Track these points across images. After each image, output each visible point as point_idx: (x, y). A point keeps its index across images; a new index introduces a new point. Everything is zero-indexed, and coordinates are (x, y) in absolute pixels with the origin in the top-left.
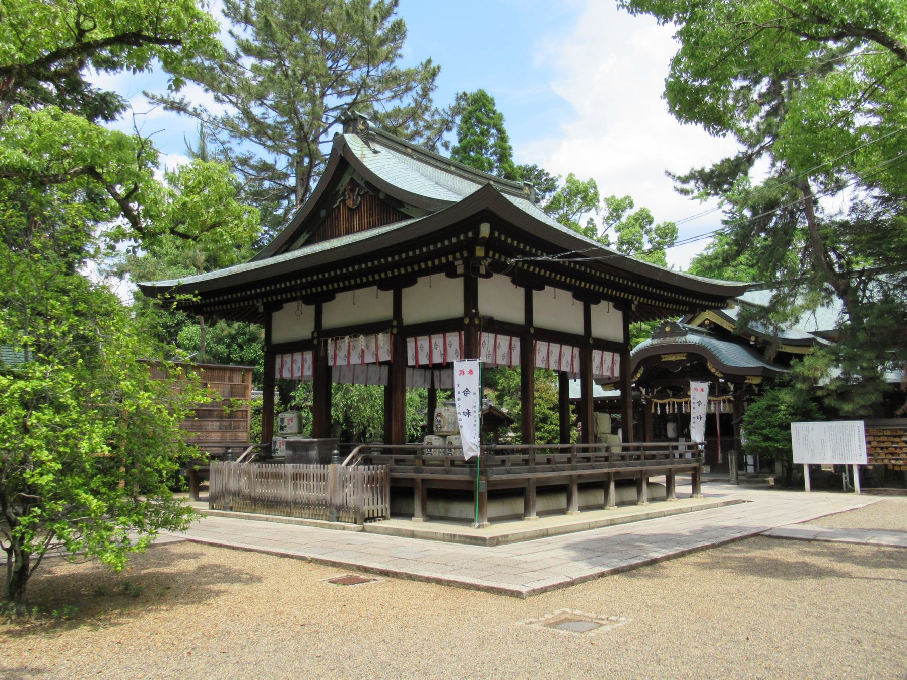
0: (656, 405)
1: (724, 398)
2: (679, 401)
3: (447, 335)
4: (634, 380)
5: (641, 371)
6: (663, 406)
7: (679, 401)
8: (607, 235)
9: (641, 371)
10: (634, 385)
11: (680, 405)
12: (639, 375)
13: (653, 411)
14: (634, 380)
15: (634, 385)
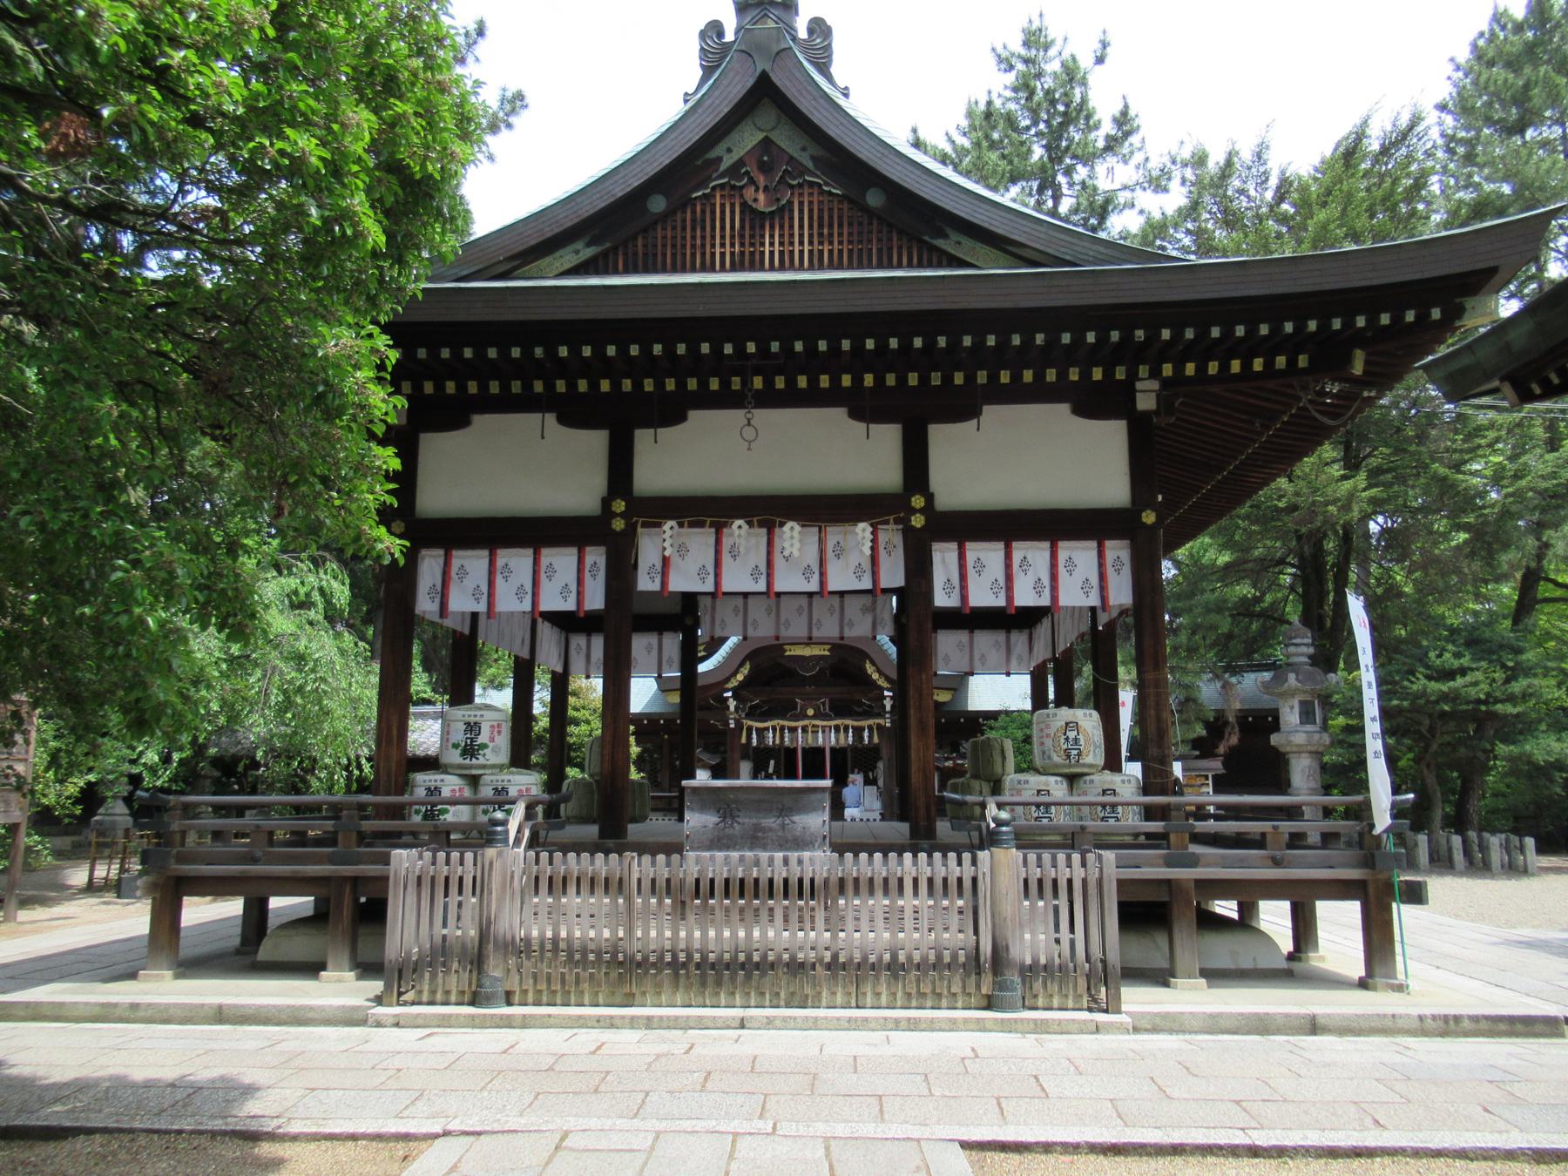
0: (750, 729)
1: (871, 722)
2: (793, 724)
3: (545, 552)
4: (730, 685)
5: (746, 670)
7: (793, 724)
13: (744, 740)
14: (730, 685)
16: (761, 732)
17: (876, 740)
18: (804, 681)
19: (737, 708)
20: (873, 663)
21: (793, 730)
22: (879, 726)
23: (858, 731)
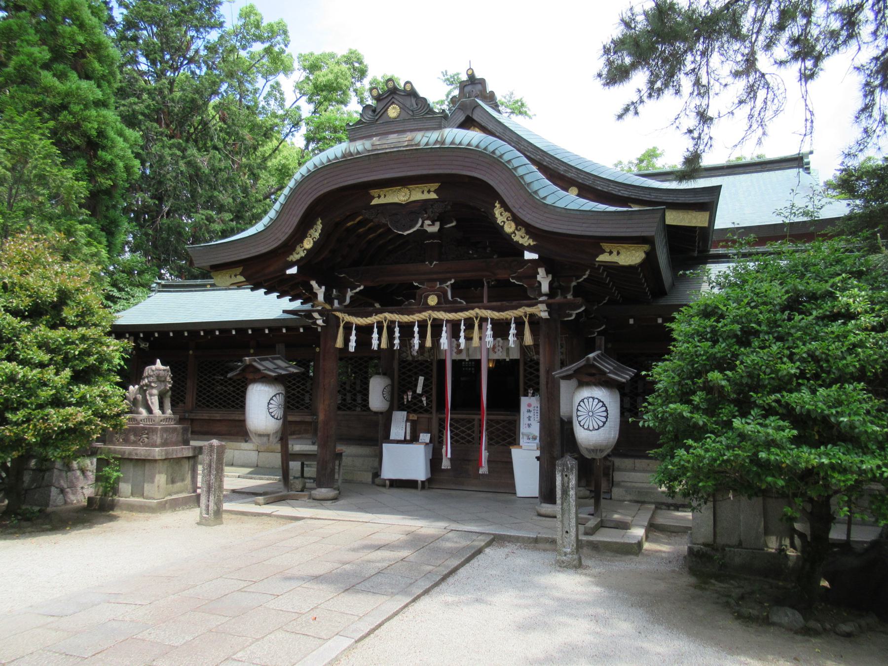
0: (348, 327)
1: (520, 312)
2: (406, 318)
4: (295, 257)
5: (316, 233)
6: (365, 332)
7: (406, 318)
8: (298, 108)
9: (316, 233)
10: (293, 270)
11: (406, 329)
12: (308, 244)
13: (339, 343)
14: (295, 257)
15: (293, 270)
16: (365, 332)
17: (528, 339)
20: (505, 207)
21: (406, 329)
22: (532, 316)
23: (501, 329)
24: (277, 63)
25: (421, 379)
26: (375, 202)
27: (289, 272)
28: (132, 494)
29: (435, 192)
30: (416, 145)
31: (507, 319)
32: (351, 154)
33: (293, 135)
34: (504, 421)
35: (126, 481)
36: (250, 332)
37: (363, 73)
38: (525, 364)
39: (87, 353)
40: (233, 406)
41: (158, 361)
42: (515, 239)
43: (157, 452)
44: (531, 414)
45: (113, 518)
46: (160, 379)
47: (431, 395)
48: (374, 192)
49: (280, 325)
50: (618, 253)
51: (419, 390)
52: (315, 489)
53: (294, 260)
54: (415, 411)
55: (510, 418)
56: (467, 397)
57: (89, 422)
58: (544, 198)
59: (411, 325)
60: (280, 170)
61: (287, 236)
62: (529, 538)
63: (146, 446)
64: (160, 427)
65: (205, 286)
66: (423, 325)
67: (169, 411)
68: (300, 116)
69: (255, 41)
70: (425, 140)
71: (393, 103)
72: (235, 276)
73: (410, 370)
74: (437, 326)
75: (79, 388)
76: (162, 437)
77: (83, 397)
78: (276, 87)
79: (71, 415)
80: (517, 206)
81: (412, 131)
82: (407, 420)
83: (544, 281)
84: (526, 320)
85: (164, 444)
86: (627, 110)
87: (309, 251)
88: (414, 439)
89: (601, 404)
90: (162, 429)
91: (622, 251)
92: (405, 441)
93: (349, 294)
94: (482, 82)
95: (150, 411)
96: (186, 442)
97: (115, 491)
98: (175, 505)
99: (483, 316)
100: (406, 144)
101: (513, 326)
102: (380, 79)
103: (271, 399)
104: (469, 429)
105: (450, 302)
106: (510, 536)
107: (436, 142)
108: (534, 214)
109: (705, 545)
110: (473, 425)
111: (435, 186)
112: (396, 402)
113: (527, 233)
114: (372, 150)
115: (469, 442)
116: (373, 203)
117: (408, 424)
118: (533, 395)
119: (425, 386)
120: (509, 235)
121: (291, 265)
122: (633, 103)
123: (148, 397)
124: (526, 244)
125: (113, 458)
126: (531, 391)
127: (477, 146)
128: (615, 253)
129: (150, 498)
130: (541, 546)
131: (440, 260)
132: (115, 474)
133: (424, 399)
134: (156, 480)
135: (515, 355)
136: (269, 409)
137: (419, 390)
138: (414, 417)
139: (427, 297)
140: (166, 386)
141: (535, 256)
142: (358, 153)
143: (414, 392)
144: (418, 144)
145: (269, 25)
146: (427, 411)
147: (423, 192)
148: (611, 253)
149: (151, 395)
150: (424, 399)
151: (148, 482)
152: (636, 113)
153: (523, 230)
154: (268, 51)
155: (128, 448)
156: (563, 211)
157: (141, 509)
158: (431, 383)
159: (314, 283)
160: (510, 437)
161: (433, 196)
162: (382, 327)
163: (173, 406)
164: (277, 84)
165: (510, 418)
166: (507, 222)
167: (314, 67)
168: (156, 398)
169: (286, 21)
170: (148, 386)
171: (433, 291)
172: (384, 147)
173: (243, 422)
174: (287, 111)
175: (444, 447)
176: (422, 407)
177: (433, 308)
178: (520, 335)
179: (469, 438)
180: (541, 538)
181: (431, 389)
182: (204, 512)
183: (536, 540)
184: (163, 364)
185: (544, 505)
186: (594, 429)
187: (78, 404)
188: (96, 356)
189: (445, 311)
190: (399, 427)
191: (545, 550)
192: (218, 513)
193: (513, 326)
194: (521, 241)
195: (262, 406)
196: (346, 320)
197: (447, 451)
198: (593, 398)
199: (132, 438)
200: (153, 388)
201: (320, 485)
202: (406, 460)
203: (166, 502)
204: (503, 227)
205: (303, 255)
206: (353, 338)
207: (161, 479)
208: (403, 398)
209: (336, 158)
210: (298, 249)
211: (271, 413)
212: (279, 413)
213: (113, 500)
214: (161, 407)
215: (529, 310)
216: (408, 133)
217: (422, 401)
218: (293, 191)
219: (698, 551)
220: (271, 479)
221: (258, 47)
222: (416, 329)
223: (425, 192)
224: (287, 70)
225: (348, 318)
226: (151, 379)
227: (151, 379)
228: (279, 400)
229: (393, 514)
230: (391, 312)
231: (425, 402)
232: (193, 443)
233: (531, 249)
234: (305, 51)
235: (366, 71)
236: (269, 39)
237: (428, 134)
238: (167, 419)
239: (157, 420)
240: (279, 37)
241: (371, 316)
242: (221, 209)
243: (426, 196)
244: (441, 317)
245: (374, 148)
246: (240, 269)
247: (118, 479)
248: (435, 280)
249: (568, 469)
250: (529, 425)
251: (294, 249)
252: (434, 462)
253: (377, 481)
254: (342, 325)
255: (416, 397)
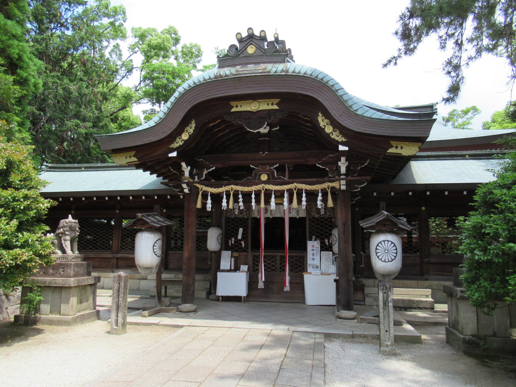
1: (325, 185)
2: (246, 189)
4: (175, 145)
5: (191, 129)
6: (217, 199)
7: (246, 189)
8: (131, 61)
9: (191, 129)
10: (174, 154)
11: (247, 196)
12: (185, 136)
13: (199, 205)
14: (175, 145)
15: (174, 154)
16: (217, 199)
17: (330, 203)
18: (257, 143)
19: (191, 173)
20: (327, 115)
21: (247, 196)
22: (333, 188)
23: (312, 196)
24: (118, 32)
25: (241, 230)
26: (234, 110)
27: (171, 155)
28: (51, 312)
29: (277, 104)
30: (268, 72)
31: (316, 190)
32: (221, 76)
33: (127, 77)
34: (296, 256)
35: (46, 302)
36: (119, 198)
37: (177, 41)
38: (310, 220)
39: (28, 208)
40: (103, 249)
41: (70, 216)
42: (333, 137)
43: (72, 281)
44: (315, 252)
45: (39, 331)
46: (71, 229)
47: (248, 240)
48: (233, 103)
49: (141, 194)
50: (402, 148)
51: (240, 237)
52: (180, 304)
53: (175, 147)
54: (236, 251)
55: (300, 254)
56: (275, 240)
57: (30, 260)
58: (356, 110)
59: (249, 194)
60: (126, 97)
61: (172, 130)
62: (348, 335)
63: (62, 277)
64: (73, 263)
65: (81, 168)
66: (258, 194)
67: (77, 252)
68: (133, 66)
69: (104, 17)
70: (274, 70)
71: (251, 44)
72: (130, 157)
73: (233, 224)
74: (268, 194)
75: (23, 235)
76: (74, 270)
77: (26, 241)
78: (117, 46)
79: (19, 254)
80: (338, 115)
81: (264, 63)
82: (232, 257)
83: (343, 165)
84: (329, 191)
85: (76, 275)
86: (390, 61)
87: (186, 141)
88: (237, 269)
89: (393, 245)
90: (74, 264)
91: (404, 146)
92: (230, 271)
93: (205, 172)
94: (283, 43)
95: (64, 251)
96: (89, 274)
97: (37, 310)
98: (83, 319)
99: (300, 188)
100: (261, 71)
101: (320, 195)
102: (188, 45)
103: (155, 243)
104: (273, 262)
105: (276, 179)
106: (335, 334)
107: (282, 71)
108: (349, 121)
109: (473, 336)
110: (276, 260)
111: (277, 101)
112: (225, 246)
113: (341, 133)
114: (236, 75)
115: (273, 270)
116: (233, 110)
117: (233, 259)
118: (315, 240)
119: (243, 234)
120: (328, 135)
121: (172, 150)
122: (394, 57)
123: (63, 242)
124: (340, 141)
125: (37, 286)
126: (314, 238)
127: (311, 75)
128: (400, 147)
129: (66, 315)
130: (356, 340)
131: (269, 151)
132: (38, 298)
133: (243, 243)
134: (71, 301)
135: (302, 214)
136: (154, 249)
137: (240, 237)
138: (236, 254)
139: (260, 175)
140: (75, 233)
141: (346, 148)
142: (226, 76)
143: (236, 238)
144: (269, 72)
145: (114, 7)
146: (244, 250)
147: (268, 105)
148: (397, 147)
149: (65, 240)
150: (243, 243)
151: (64, 303)
152: (396, 64)
153: (338, 131)
154: (112, 24)
155: (48, 279)
156: (369, 119)
157: (59, 323)
158: (248, 232)
159: (184, 164)
160: (300, 266)
161: (276, 107)
162: (230, 195)
163: (79, 249)
164: (118, 44)
165: (300, 254)
166: (327, 126)
167: (142, 37)
168: (69, 242)
169: (124, 6)
170: (64, 234)
171: (265, 172)
172: (245, 72)
173: (133, 259)
174: (124, 62)
175: (260, 274)
176: (241, 248)
177: (265, 182)
178: (325, 200)
179: (273, 268)
180: (356, 335)
181: (248, 236)
182: (114, 324)
183: (353, 336)
184: (73, 218)
185: (343, 311)
186: (389, 261)
187: (22, 247)
188: (35, 211)
189: (273, 184)
190: (226, 261)
191: (361, 343)
192: (124, 324)
193: (320, 195)
194: (337, 138)
195: (147, 248)
196: (203, 189)
197: (262, 277)
198: (388, 241)
199: (51, 271)
200: (66, 235)
201: (185, 301)
202: (233, 282)
203: (77, 317)
204: (324, 129)
205: (181, 144)
206: (209, 201)
207: (74, 300)
208: (228, 242)
209: (210, 78)
210: (178, 139)
211: (154, 252)
212: (159, 252)
213: (36, 317)
214: (72, 250)
215: (331, 184)
216: (262, 65)
217: (241, 244)
218: (178, 100)
219: (469, 340)
220: (134, 297)
221: (106, 21)
222: (253, 196)
223: (270, 105)
224: (124, 37)
225: (205, 188)
226: (65, 229)
227: (65, 229)
228: (159, 243)
229: (243, 321)
230: (237, 185)
231: (243, 245)
232: (94, 274)
233: (343, 144)
234: (136, 26)
235: (179, 40)
236: (114, 16)
237: (277, 65)
238: (76, 257)
239: (70, 258)
240: (120, 16)
241: (221, 187)
242: (84, 120)
243: (270, 107)
244: (271, 188)
245: (238, 73)
246: (133, 153)
247: (40, 302)
248: (267, 164)
249: (386, 288)
250: (313, 259)
251: (174, 140)
252: (252, 283)
253: (211, 297)
254: (200, 193)
255: (238, 242)
